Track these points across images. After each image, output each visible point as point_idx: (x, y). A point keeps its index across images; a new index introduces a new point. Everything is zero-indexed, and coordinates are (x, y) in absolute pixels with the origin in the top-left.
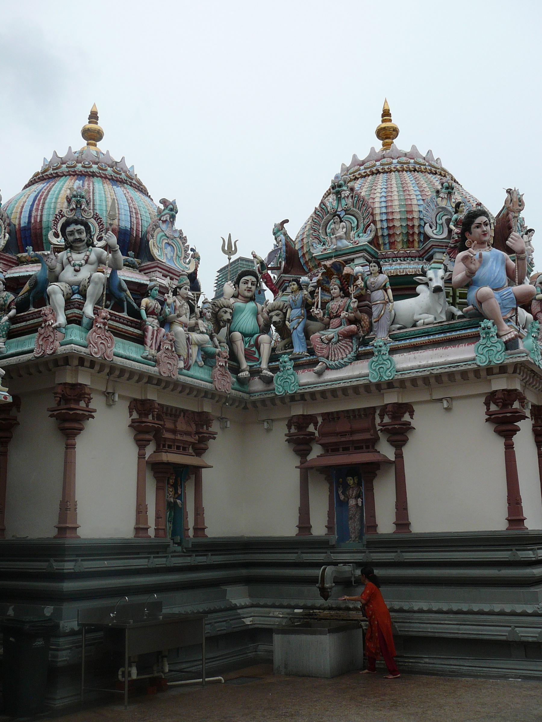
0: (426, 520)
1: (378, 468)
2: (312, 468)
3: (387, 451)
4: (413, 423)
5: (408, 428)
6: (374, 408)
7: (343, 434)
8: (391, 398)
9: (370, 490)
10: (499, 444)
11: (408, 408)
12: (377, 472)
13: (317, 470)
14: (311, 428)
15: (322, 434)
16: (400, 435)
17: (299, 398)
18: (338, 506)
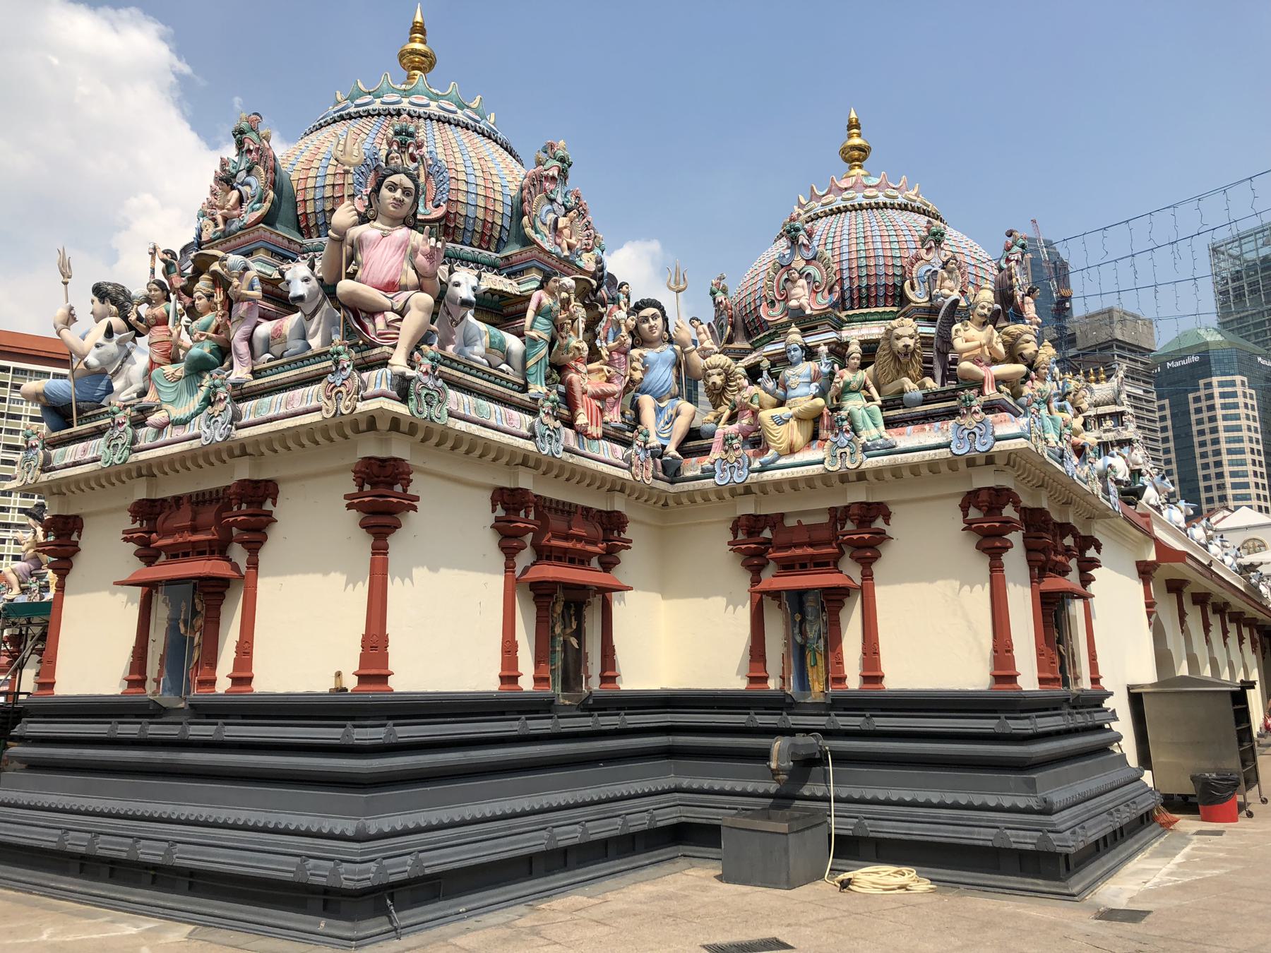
5: (269, 519)
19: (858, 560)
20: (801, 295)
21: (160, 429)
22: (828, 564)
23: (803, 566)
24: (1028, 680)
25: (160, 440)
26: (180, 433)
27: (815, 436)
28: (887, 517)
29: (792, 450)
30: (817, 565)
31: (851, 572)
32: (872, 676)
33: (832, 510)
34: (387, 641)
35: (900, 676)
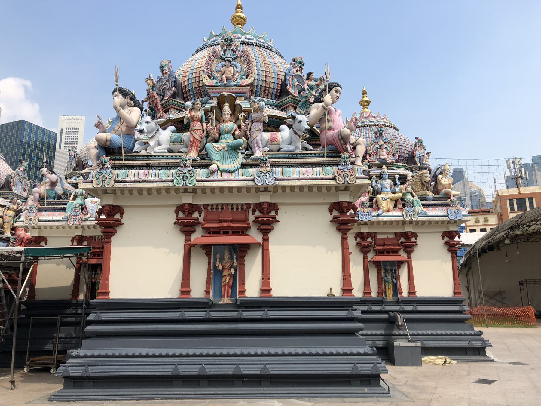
0: (280, 289)
1: (249, 248)
2: (194, 245)
3: (255, 236)
4: (277, 218)
5: (274, 220)
6: (248, 205)
7: (226, 221)
8: (265, 198)
9: (242, 263)
10: (338, 237)
11: (274, 207)
12: (248, 251)
13: (201, 247)
14: (196, 215)
15: (206, 220)
16: (266, 226)
17: (191, 190)
18: (215, 274)
19: (406, 251)
20: (384, 155)
21: (212, 173)
22: (395, 252)
23: (388, 253)
24: (358, 293)
25: (212, 178)
26: (226, 176)
27: (395, 206)
28: (416, 237)
29: (388, 211)
30: (393, 252)
31: (403, 256)
32: (412, 292)
33: (396, 234)
34: (350, 276)
35: (421, 292)
